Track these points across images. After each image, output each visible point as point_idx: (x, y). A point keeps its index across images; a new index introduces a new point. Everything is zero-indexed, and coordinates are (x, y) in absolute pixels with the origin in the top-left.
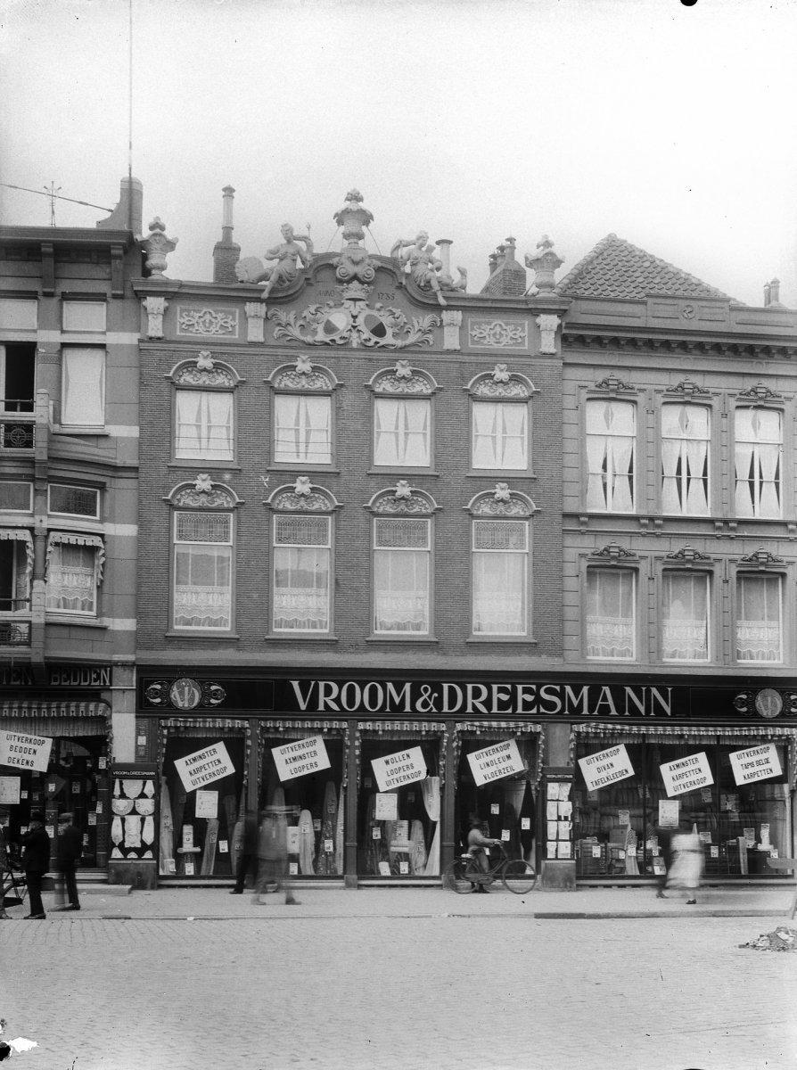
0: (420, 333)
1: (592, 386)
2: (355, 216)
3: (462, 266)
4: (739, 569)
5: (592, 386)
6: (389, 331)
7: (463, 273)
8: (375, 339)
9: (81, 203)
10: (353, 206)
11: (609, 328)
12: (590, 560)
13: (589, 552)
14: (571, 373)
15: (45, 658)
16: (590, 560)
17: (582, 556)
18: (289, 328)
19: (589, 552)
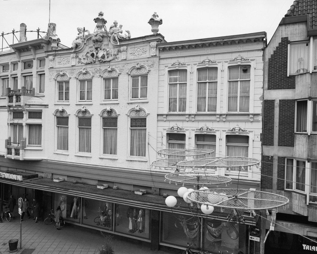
1: (170, 66)
2: (100, 21)
3: (127, 30)
4: (227, 134)
5: (170, 66)
6: (106, 56)
7: (128, 32)
8: (102, 60)
9: (43, 32)
10: (100, 17)
12: (167, 131)
14: (162, 62)
15: (24, 159)
16: (167, 131)
17: (164, 129)
18: (81, 60)
19: (167, 128)
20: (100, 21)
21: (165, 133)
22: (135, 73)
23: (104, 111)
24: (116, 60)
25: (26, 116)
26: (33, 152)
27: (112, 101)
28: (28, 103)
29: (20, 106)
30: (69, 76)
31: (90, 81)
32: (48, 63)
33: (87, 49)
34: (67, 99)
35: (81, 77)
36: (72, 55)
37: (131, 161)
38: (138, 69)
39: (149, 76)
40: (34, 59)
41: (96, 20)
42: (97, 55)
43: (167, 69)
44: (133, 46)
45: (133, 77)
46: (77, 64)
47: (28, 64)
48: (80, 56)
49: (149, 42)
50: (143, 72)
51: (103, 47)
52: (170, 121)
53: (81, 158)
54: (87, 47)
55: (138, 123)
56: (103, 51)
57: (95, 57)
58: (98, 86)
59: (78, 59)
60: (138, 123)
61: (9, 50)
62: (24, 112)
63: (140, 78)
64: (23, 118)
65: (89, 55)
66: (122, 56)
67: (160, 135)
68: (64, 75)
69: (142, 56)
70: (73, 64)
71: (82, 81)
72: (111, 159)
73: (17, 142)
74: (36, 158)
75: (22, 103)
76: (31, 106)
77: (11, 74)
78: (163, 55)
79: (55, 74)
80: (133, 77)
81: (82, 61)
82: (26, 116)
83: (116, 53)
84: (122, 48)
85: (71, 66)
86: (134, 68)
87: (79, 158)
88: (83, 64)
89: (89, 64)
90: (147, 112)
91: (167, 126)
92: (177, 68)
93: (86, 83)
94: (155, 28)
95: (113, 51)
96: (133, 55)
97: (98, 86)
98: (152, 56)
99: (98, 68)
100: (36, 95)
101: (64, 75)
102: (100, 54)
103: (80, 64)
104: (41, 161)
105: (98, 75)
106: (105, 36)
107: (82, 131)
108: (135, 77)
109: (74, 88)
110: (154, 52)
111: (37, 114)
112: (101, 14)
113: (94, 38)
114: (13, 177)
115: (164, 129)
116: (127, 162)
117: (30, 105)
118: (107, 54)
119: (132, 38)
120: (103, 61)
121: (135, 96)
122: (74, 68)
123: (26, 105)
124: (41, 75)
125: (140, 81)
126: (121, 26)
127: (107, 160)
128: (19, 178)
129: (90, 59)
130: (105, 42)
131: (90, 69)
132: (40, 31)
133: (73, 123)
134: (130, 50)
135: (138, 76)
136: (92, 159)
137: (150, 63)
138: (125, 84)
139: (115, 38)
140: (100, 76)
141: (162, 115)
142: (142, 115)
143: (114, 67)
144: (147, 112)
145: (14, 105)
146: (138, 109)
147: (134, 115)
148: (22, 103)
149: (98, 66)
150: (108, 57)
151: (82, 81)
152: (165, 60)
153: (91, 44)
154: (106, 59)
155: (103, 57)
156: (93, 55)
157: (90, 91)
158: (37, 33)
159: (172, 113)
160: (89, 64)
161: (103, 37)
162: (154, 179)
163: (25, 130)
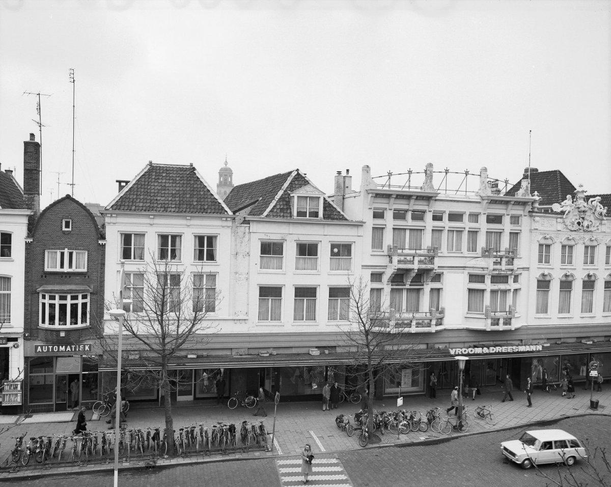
24: (597, 231)
26: (472, 319)
27: (590, 266)
34: (547, 262)
47: (495, 219)
53: (563, 319)
58: (579, 253)
65: (576, 223)
72: (591, 317)
73: (507, 310)
74: (478, 328)
75: (515, 267)
79: (540, 237)
85: (555, 230)
93: (567, 249)
97: (579, 253)
99: (582, 236)
102: (586, 223)
105: (582, 242)
109: (556, 252)
114: (533, 348)
116: (603, 318)
120: (587, 230)
122: (559, 232)
124: (514, 235)
127: (587, 319)
128: (540, 348)
129: (576, 227)
131: (574, 235)
132: (509, 182)
133: (555, 287)
136: (596, 318)
148: (515, 267)
149: (582, 234)
154: (590, 229)
155: (588, 227)
156: (579, 223)
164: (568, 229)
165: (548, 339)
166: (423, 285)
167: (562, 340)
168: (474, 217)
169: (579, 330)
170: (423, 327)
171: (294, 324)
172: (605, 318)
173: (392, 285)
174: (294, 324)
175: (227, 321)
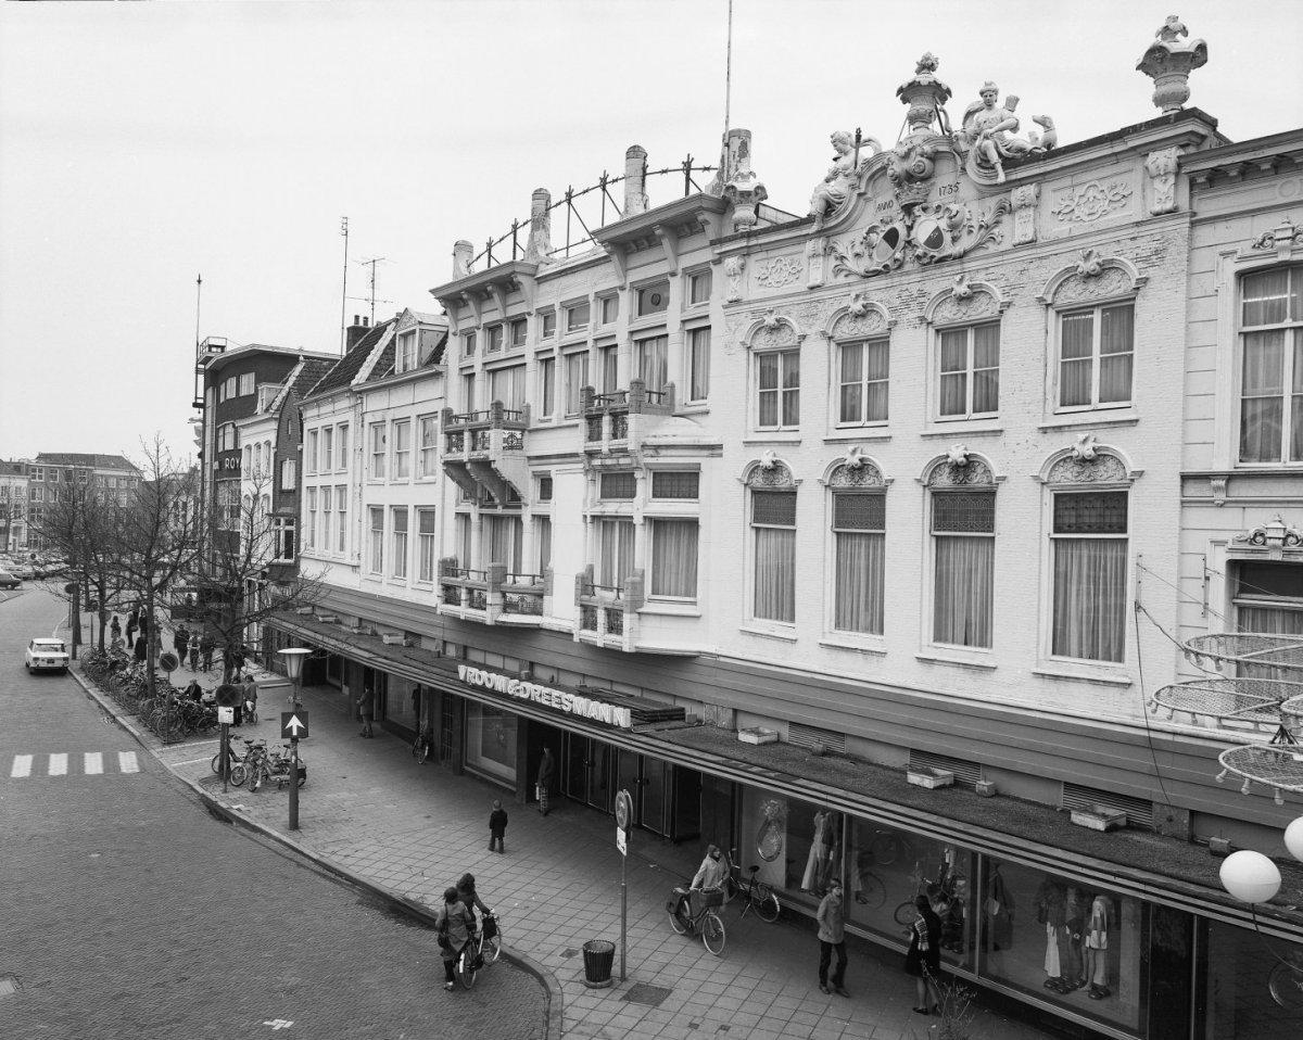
0: (983, 231)
2: (924, 93)
3: (1039, 115)
6: (947, 237)
7: (1044, 122)
8: (933, 252)
10: (924, 79)
11: (1262, 143)
12: (1231, 550)
13: (1229, 536)
14: (1205, 234)
15: (636, 647)
16: (1231, 550)
17: (1217, 543)
18: (845, 261)
19: (1229, 536)
20: (924, 93)
21: (1219, 561)
22: (1074, 294)
23: (937, 466)
24: (992, 248)
25: (644, 487)
26: (666, 623)
27: (973, 421)
28: (651, 441)
29: (624, 451)
30: (798, 332)
31: (881, 344)
32: (723, 286)
33: (869, 216)
34: (791, 418)
35: (847, 330)
36: (810, 246)
37: (1056, 678)
38: (1089, 276)
39: (1139, 303)
40: (673, 274)
41: (908, 93)
42: (909, 235)
43: (1232, 267)
44: (1067, 181)
45: (1066, 313)
46: (832, 281)
47: (652, 297)
48: (843, 244)
49: (1142, 152)
50: (1112, 288)
51: (935, 199)
52: (1244, 504)
53: (844, 656)
54: (871, 208)
55: (1092, 513)
56: (934, 217)
57: (901, 244)
59: (832, 258)
60: (1092, 513)
61: (588, 250)
62: (638, 475)
63: (1097, 317)
64: (633, 495)
65: (877, 238)
66: (1017, 229)
67: (1194, 567)
68: (780, 326)
69: (1103, 223)
70: (816, 279)
71: (849, 347)
72: (966, 666)
73: (616, 585)
75: (630, 442)
76: (663, 452)
77: (632, 329)
78: (1209, 206)
79: (748, 323)
80: (1066, 313)
81: (851, 264)
82: (644, 487)
83: (989, 218)
84: (1016, 196)
85: (804, 289)
86: (1069, 275)
87: (835, 653)
88: (852, 279)
89: (877, 273)
90: (1132, 465)
91: (1230, 528)
92: (1285, 257)
93: (865, 351)
94: (1171, 87)
95: (974, 210)
96: (1068, 217)
97: (914, 362)
98: (1157, 214)
100: (678, 410)
101: (780, 326)
102: (924, 229)
103: (841, 279)
104: (695, 657)
105: (913, 315)
106: (945, 152)
107: (847, 544)
108: (1073, 319)
110: (1165, 193)
111: (680, 482)
112: (927, 66)
113: (898, 168)
115: (1217, 543)
116: (1038, 682)
117: (657, 448)
118: (953, 227)
119: (1060, 144)
120: (934, 258)
121: (1074, 395)
122: (817, 295)
123: (644, 446)
124: (698, 332)
125: (1097, 328)
126: (1012, 103)
127: (951, 671)
128: (621, 717)
129: (883, 255)
130: (945, 175)
131: (881, 293)
132: (693, 166)
134: (1054, 197)
135: (1089, 309)
136: (885, 661)
137: (1146, 246)
138: (1028, 350)
139: (985, 155)
140: (922, 319)
141: (1205, 477)
142: (1106, 477)
143: (980, 279)
144: (1132, 465)
145: (605, 449)
146: (1087, 451)
147: (1068, 478)
148: (630, 442)
149: (911, 281)
150: (954, 240)
151: (849, 347)
152: (1221, 226)
153: (886, 192)
154: (948, 249)
155: (935, 241)
156: (892, 237)
157: (879, 387)
158: (682, 176)
159: (1254, 465)
160: (877, 273)
161: (934, 157)
162: (1166, 765)
163: (643, 538)
164: (850, 273)
165: (792, 724)
166: (520, 507)
167: (849, 742)
168: (608, 299)
169: (905, 715)
170: (523, 613)
171: (394, 582)
172: (1052, 686)
173: (481, 507)
174: (394, 582)
175: (663, 619)
